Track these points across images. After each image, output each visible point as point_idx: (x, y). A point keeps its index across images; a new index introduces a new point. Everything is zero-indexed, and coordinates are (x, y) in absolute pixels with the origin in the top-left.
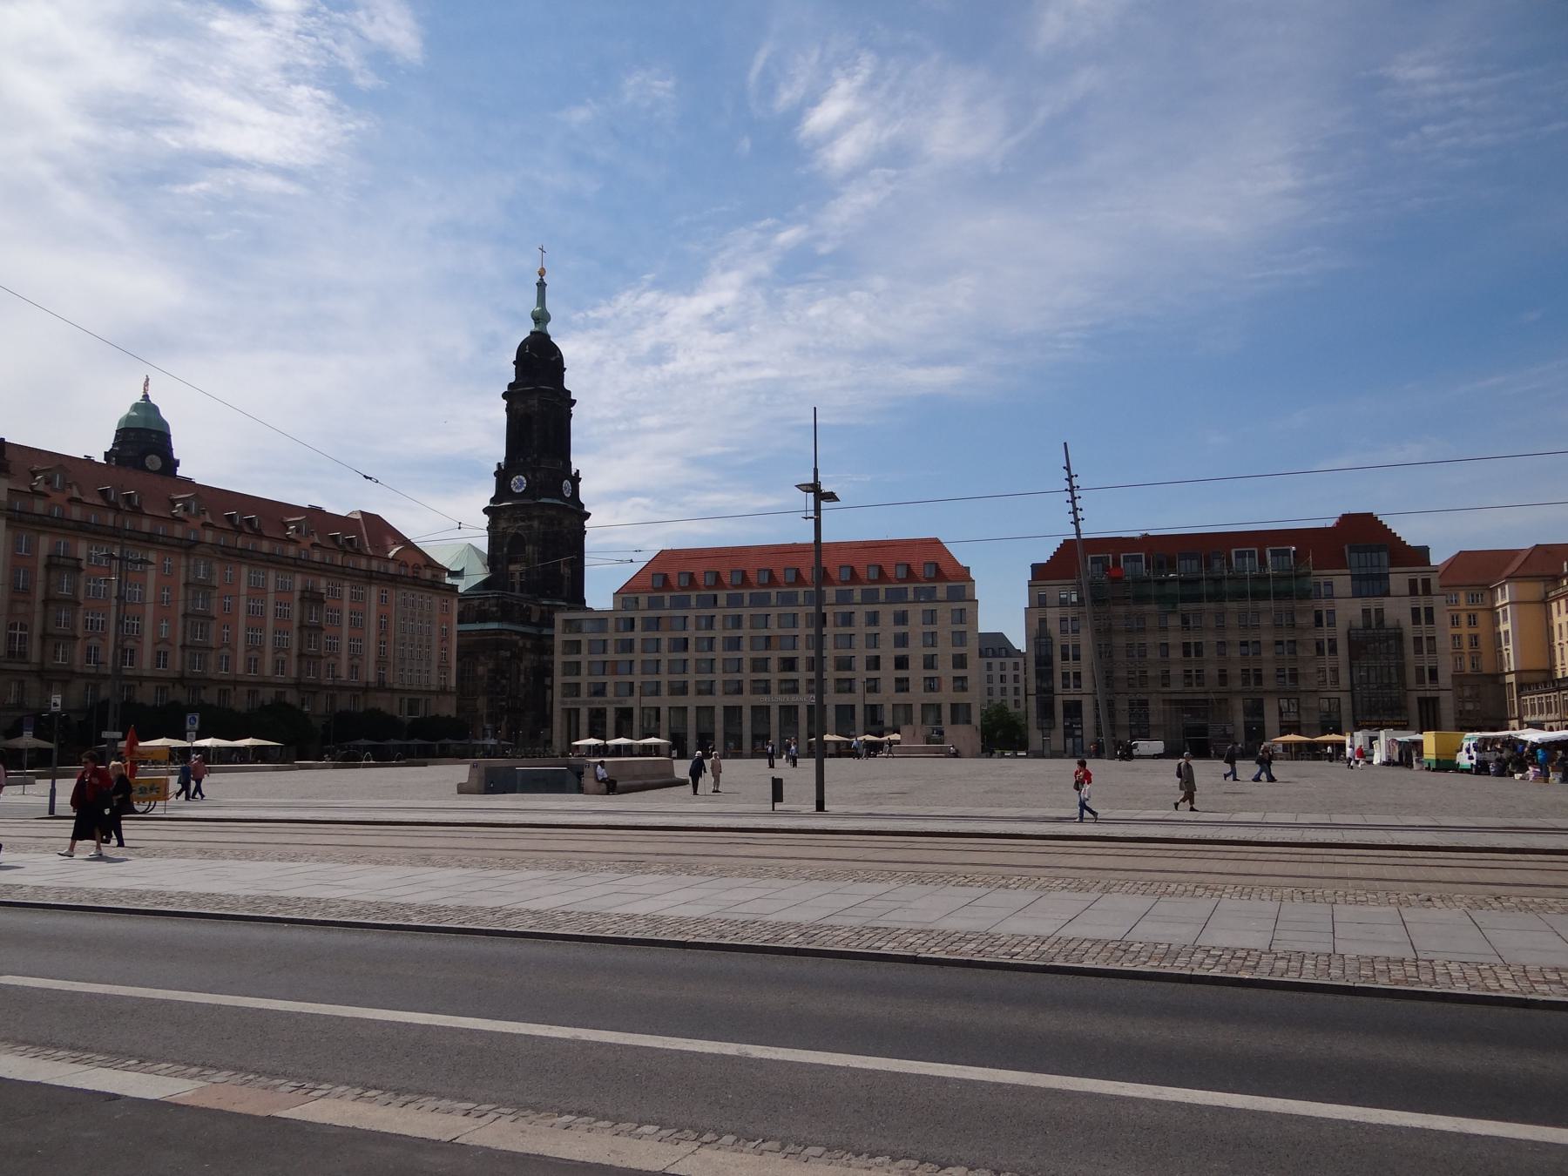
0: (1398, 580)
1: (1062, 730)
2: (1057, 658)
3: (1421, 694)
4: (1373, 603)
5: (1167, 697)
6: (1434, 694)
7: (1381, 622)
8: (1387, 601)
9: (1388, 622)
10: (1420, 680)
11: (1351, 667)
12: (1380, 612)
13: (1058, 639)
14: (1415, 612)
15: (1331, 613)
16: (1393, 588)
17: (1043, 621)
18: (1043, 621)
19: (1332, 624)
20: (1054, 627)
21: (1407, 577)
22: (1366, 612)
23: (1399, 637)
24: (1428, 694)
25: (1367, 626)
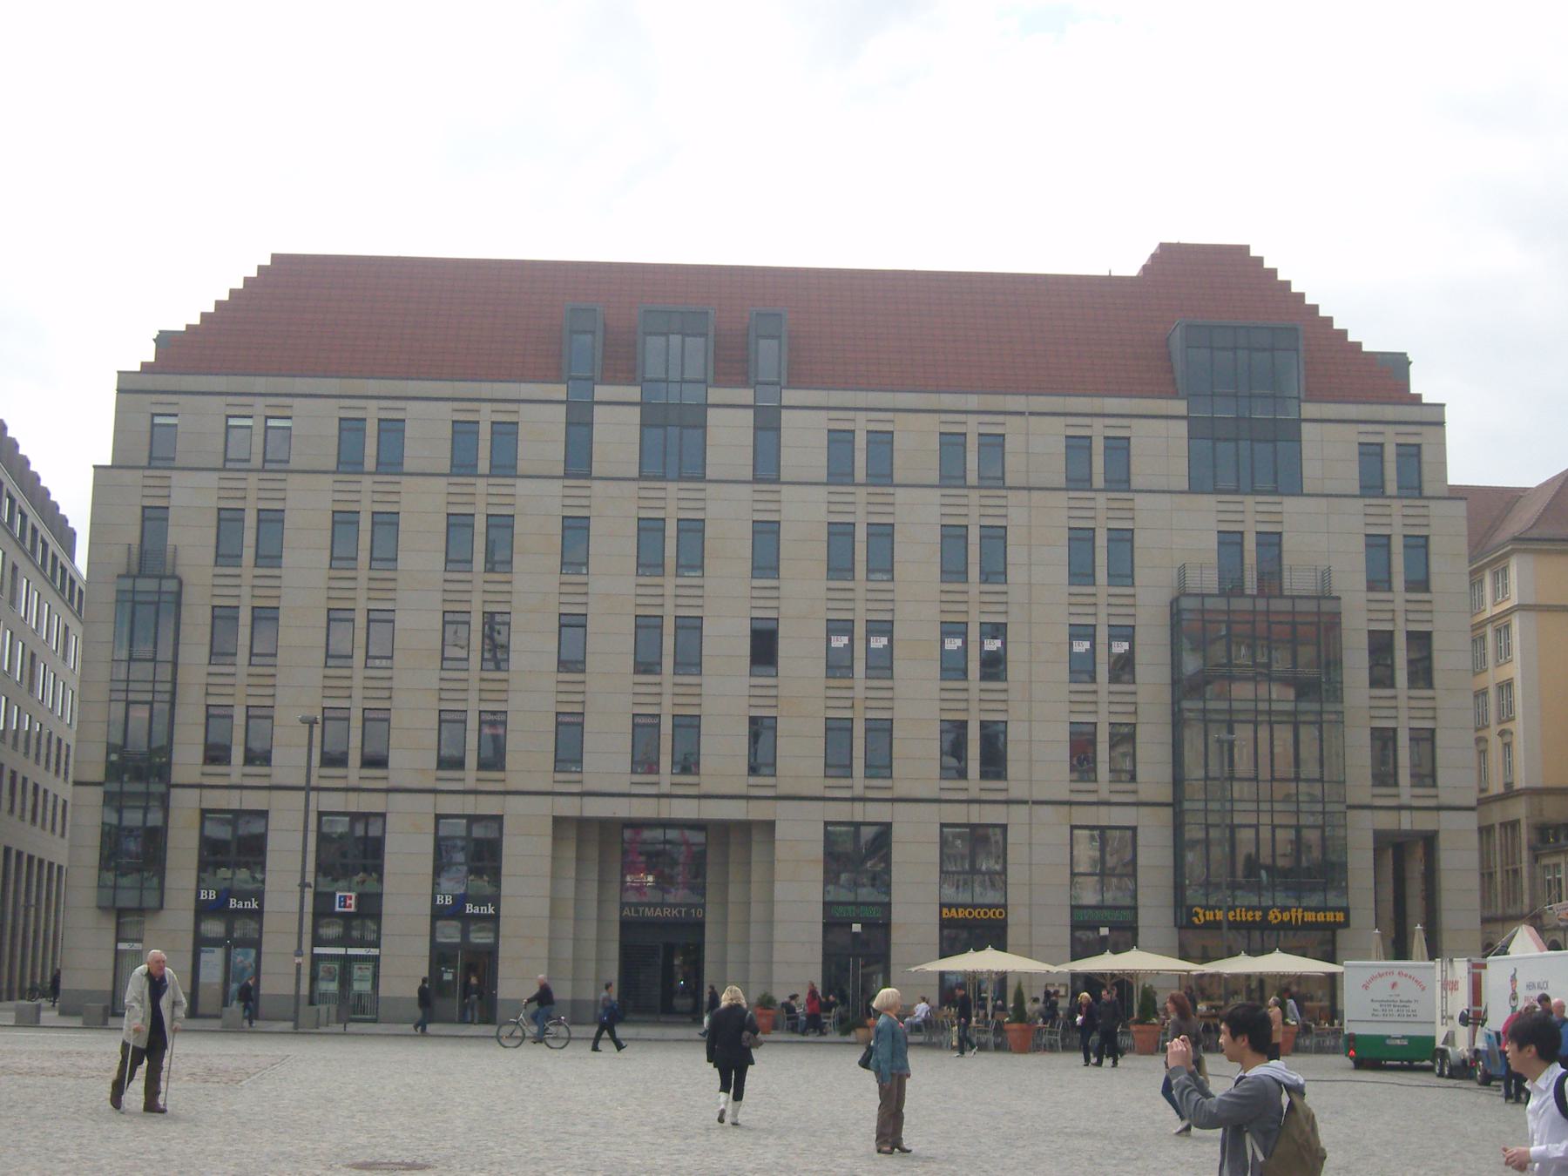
0: (1328, 445)
1: (188, 918)
2: (195, 651)
3: (1386, 821)
4: (1251, 514)
5: (569, 808)
6: (1423, 822)
7: (1271, 575)
8: (1290, 504)
9: (1298, 581)
10: (1385, 776)
11: (1178, 723)
12: (1271, 542)
13: (201, 579)
14: (1378, 545)
15: (1123, 540)
16: (1311, 470)
17: (154, 518)
18: (154, 518)
19: (1123, 574)
20: (192, 544)
21: (1351, 436)
22: (1230, 541)
23: (1327, 625)
24: (1407, 822)
25: (1231, 587)
